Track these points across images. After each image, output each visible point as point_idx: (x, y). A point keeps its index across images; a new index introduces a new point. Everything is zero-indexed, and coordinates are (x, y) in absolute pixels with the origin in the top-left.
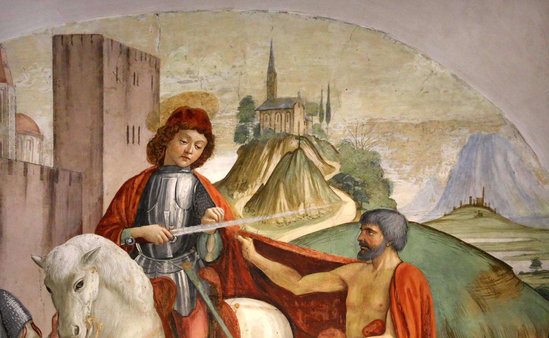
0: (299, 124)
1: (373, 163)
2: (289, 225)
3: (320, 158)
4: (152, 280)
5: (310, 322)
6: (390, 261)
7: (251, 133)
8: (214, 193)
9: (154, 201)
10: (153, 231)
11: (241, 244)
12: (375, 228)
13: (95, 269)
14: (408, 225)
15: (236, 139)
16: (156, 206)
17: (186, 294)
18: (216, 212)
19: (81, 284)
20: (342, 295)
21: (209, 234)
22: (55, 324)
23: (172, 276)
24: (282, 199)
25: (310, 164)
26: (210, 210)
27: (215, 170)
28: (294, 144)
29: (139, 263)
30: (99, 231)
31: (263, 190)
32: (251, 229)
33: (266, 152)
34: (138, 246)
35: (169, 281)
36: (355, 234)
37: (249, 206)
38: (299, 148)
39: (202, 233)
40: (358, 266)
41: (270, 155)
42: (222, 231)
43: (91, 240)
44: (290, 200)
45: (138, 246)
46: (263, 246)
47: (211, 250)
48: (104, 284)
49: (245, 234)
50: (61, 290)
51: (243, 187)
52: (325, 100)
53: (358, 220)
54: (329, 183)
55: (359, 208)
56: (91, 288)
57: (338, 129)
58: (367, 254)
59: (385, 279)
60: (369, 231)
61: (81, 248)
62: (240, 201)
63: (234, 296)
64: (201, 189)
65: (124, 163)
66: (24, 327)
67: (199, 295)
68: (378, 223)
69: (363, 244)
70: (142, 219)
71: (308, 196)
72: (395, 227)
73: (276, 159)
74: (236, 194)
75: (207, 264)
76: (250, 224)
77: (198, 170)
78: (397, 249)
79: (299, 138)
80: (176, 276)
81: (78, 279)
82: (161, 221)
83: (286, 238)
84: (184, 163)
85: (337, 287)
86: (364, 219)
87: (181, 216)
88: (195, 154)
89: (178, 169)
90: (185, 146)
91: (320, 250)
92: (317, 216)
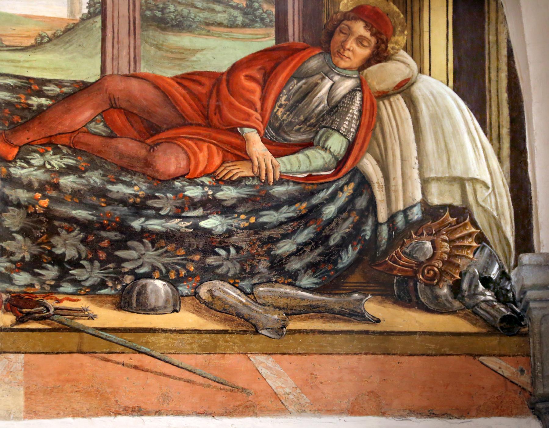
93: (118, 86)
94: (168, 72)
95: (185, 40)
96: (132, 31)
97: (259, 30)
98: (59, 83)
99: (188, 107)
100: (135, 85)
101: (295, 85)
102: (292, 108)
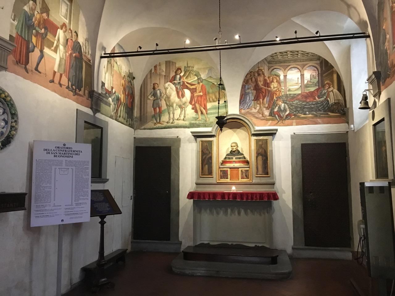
0: (191, 69)
1: (199, 73)
2: (190, 80)
5: (193, 91)
6: (201, 84)
8: (182, 77)
17: (179, 89)
19: (168, 88)
20: (196, 88)
22: (165, 93)
24: (189, 77)
25: (192, 73)
27: (182, 74)
28: (190, 71)
36: (197, 81)
37: (186, 78)
42: (183, 81)
43: (169, 83)
46: (187, 83)
47: (182, 84)
48: (170, 88)
50: (166, 89)
57: (195, 69)
58: (199, 83)
59: (201, 86)
64: (180, 76)
65: (172, 74)
69: (198, 82)
70: (174, 80)
72: (201, 80)
73: (188, 73)
76: (186, 80)
78: (202, 82)
82: (176, 80)
83: (189, 82)
85: (195, 87)
86: (198, 79)
87: (178, 80)
88: (180, 73)
89: (178, 74)
91: (193, 83)
92: (193, 79)
93: (303, 94)
94: (307, 92)
95: (309, 88)
96: (304, 88)
97: (317, 87)
98: (297, 94)
99: (310, 95)
100: (304, 93)
101: (320, 92)
102: (320, 94)
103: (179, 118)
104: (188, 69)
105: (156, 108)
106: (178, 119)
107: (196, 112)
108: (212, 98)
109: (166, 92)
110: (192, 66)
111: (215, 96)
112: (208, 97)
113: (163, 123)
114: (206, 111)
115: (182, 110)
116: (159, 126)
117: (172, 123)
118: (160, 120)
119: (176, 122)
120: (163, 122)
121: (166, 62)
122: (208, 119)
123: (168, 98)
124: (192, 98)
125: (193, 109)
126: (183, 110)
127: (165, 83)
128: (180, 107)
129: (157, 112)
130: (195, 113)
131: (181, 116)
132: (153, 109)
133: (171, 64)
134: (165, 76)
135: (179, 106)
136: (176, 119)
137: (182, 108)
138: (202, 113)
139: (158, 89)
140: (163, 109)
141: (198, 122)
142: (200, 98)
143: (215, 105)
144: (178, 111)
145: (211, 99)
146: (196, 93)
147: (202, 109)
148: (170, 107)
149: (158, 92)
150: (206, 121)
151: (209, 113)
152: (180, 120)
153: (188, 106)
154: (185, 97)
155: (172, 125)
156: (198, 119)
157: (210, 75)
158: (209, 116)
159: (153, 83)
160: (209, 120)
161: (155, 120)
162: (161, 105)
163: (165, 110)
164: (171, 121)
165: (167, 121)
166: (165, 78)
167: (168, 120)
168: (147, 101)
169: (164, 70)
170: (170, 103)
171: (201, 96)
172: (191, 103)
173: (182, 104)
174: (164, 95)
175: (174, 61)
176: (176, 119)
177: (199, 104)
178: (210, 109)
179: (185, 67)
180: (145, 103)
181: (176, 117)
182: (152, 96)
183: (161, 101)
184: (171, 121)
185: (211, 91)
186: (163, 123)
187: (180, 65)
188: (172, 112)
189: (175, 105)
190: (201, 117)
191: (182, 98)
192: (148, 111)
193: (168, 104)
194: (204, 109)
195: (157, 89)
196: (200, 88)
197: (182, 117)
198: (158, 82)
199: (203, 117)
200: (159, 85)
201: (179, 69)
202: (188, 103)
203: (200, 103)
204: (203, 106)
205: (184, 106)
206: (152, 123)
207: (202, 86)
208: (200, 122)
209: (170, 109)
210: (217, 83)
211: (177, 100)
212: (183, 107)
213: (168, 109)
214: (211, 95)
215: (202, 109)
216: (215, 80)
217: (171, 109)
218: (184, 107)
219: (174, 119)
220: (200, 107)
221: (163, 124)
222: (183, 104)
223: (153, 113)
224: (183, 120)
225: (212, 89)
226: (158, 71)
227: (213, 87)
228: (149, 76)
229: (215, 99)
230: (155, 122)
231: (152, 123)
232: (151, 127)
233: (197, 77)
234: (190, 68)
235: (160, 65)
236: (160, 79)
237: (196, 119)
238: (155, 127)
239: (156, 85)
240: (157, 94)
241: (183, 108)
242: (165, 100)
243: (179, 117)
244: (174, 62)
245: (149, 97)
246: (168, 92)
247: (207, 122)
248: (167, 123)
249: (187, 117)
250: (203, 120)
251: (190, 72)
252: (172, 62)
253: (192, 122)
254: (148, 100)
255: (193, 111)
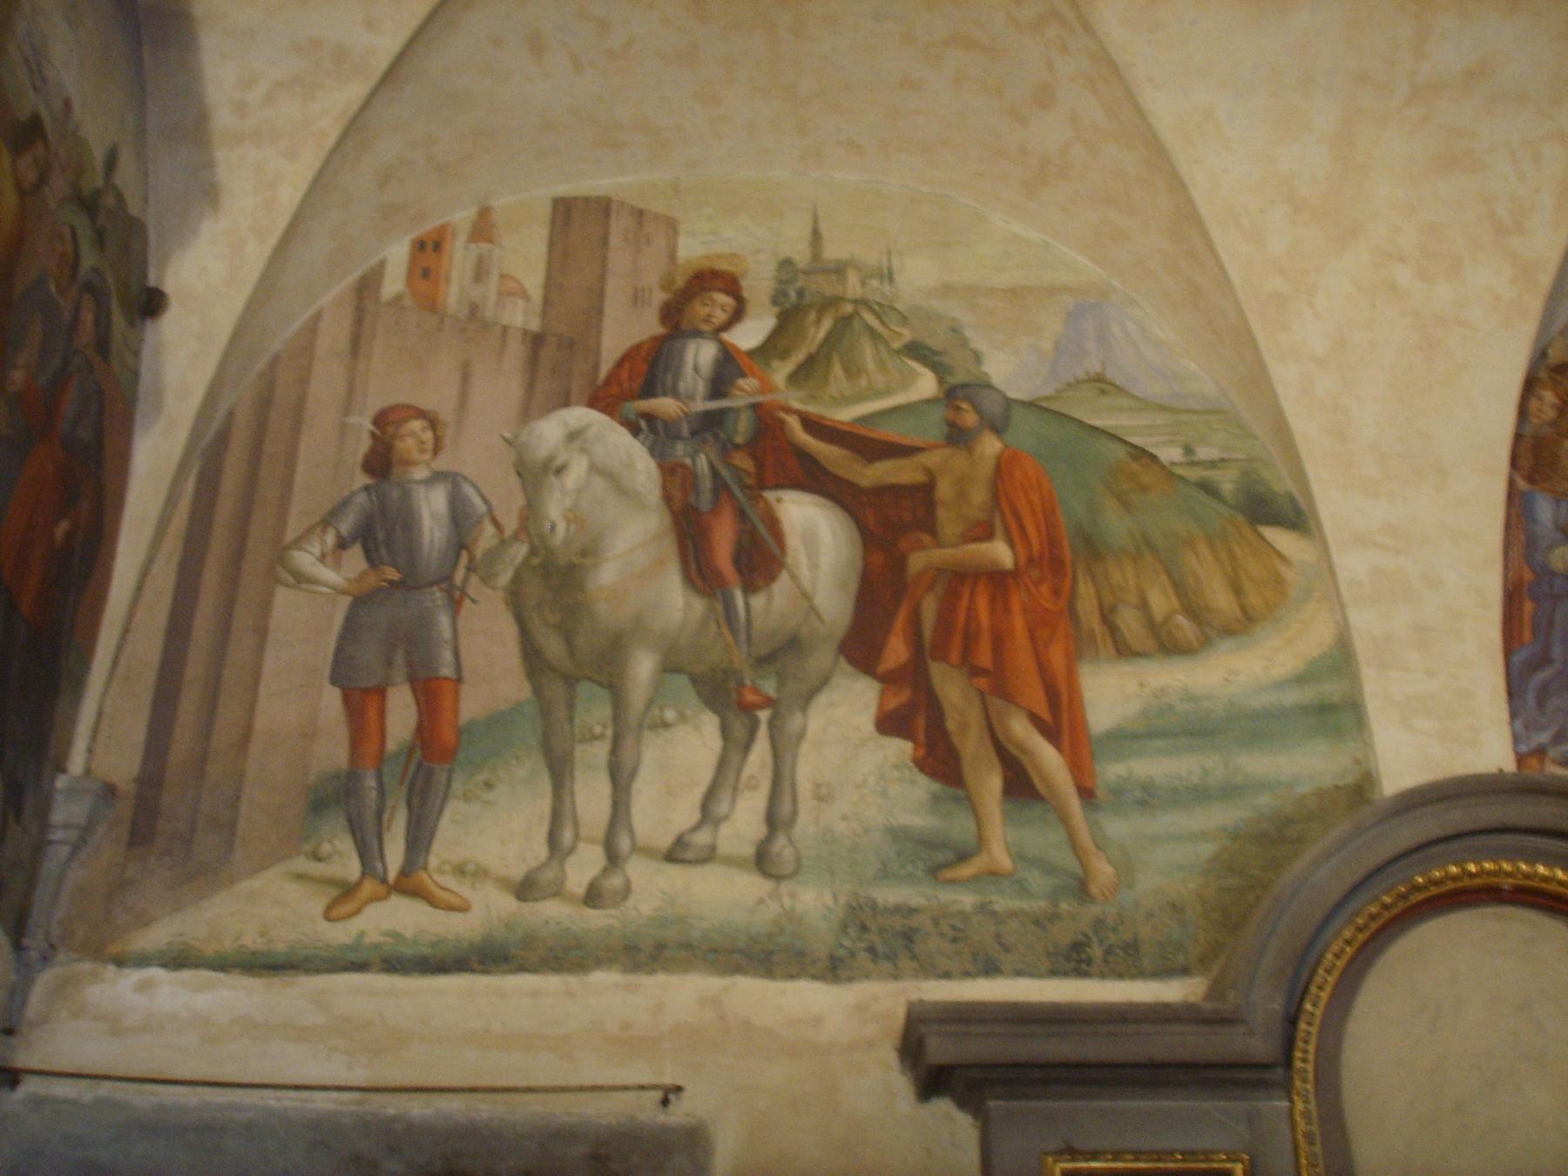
2: (848, 401)
3: (883, 323)
4: (661, 467)
6: (990, 446)
7: (793, 295)
9: (667, 370)
10: (665, 405)
11: (782, 422)
12: (964, 406)
13: (583, 450)
14: (1009, 403)
15: (774, 302)
16: (669, 376)
17: (706, 484)
18: (748, 383)
19: (560, 471)
21: (736, 411)
23: (688, 461)
24: (837, 369)
25: (872, 332)
26: (741, 382)
27: (748, 335)
28: (848, 308)
29: (643, 443)
30: (593, 403)
31: (811, 360)
32: (796, 405)
33: (812, 316)
34: (643, 424)
35: (683, 466)
36: (938, 415)
37: (794, 378)
38: (856, 313)
39: (730, 409)
40: (947, 451)
41: (818, 322)
42: (756, 407)
43: (579, 415)
44: (847, 370)
45: (643, 424)
46: (810, 424)
47: (742, 428)
48: (594, 468)
49: (789, 410)
50: (534, 475)
51: (784, 355)
52: (885, 262)
53: (942, 396)
54: (898, 352)
55: (941, 381)
56: (578, 470)
58: (957, 437)
59: (985, 469)
60: (958, 409)
61: (565, 423)
62: (780, 372)
63: (778, 486)
65: (625, 327)
66: (479, 522)
67: (725, 486)
68: (968, 399)
69: (951, 424)
70: (649, 391)
71: (871, 366)
72: (992, 406)
73: (827, 324)
74: (775, 363)
75: (737, 447)
77: (725, 336)
78: (998, 430)
79: (856, 302)
80: (694, 461)
81: (559, 462)
82: (675, 394)
83: (845, 415)
84: (705, 327)
85: (919, 477)
86: (952, 395)
87: (701, 388)
88: (720, 317)
89: (698, 334)
90: (707, 310)
91: (889, 432)
103: (702, 838)
104: (824, 285)
105: (380, 692)
106: (680, 842)
107: (940, 762)
108: (1144, 606)
109: (531, 513)
110: (871, 258)
111: (1179, 588)
112: (1086, 590)
113: (463, 889)
114: (1078, 767)
115: (739, 732)
116: (396, 935)
117: (593, 897)
118: (419, 839)
119: (652, 889)
120: (460, 871)
121: (564, 211)
122: (1103, 870)
123: (553, 580)
124: (879, 589)
125: (890, 724)
126: (763, 732)
127: (529, 411)
128: (725, 695)
129: (391, 746)
130: (924, 786)
131: (722, 807)
132: (332, 698)
133: (619, 226)
134: (536, 342)
135: (695, 681)
136: (648, 852)
137: (748, 710)
138: (1021, 785)
139: (437, 477)
140: (472, 705)
141: (967, 900)
142: (983, 605)
143: (1189, 696)
144: (689, 746)
145: (1129, 621)
146: (926, 539)
147: (1020, 729)
148: (570, 681)
149: (432, 507)
150: (1081, 888)
151: (1118, 791)
152: (708, 856)
153: (824, 682)
154: (784, 577)
155: (596, 918)
156: (963, 857)
157: (1094, 366)
158: (1116, 827)
159: (375, 404)
160: (1126, 870)
161: (346, 844)
162: (448, 656)
163: (498, 722)
164: (584, 866)
165: (518, 872)
166: (533, 362)
167: (542, 851)
168: (266, 605)
169: (533, 281)
170: (580, 641)
171: (998, 580)
172: (861, 648)
173: (740, 658)
174: (503, 542)
175: (656, 206)
176: (648, 852)
177: (976, 672)
178: (1125, 739)
179: (786, 264)
180: (243, 617)
181: (660, 809)
182: (342, 545)
183: (455, 604)
184: (584, 866)
185: (1116, 526)
186: (463, 889)
187: (721, 248)
188: (599, 752)
189: (643, 667)
190: (1002, 837)
191: (750, 588)
192: (260, 722)
193: (553, 647)
194: (1051, 733)
195: (420, 473)
196: (979, 495)
197: (744, 821)
198: (437, 395)
199: (1044, 839)
200: (449, 435)
201: (713, 279)
202: (823, 657)
203: (985, 659)
204: (1035, 697)
205: (769, 687)
206: (293, 890)
207: (1002, 469)
208: (1002, 903)
209: (571, 706)
210: (1188, 450)
211: (675, 602)
212: (750, 698)
213: (545, 712)
214: (1122, 575)
215: (1020, 729)
216: (1162, 419)
217: (594, 711)
218: (769, 702)
219: (624, 843)
220: (996, 703)
221: (462, 908)
222: (764, 661)
223: (333, 752)
224: (762, 861)
225: (1126, 505)
226: (453, 296)
227: (1144, 489)
228: (335, 333)
229: (1181, 619)
230: (351, 868)
231: (301, 877)
232: (282, 942)
233: (940, 370)
234: (853, 279)
235: (483, 229)
236: (466, 377)
237: (940, 857)
238: (340, 934)
239: (416, 425)
240: (407, 522)
241: (764, 715)
242: (515, 600)
243: (696, 816)
244: (657, 218)
245: (305, 560)
246: (555, 509)
247: (1096, 910)
248: (525, 889)
249: (806, 826)
250: (1037, 881)
251: (844, 324)
252: (640, 214)
253: (889, 895)
254: (283, 596)
255: (899, 749)
